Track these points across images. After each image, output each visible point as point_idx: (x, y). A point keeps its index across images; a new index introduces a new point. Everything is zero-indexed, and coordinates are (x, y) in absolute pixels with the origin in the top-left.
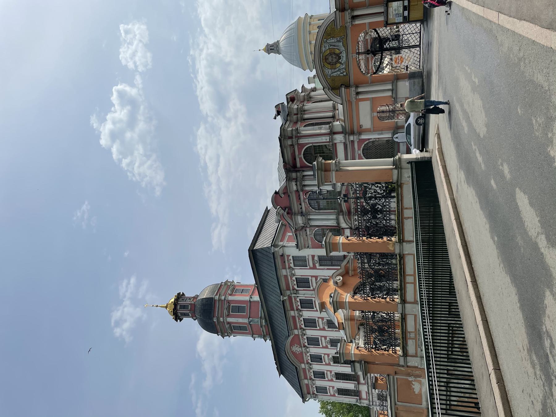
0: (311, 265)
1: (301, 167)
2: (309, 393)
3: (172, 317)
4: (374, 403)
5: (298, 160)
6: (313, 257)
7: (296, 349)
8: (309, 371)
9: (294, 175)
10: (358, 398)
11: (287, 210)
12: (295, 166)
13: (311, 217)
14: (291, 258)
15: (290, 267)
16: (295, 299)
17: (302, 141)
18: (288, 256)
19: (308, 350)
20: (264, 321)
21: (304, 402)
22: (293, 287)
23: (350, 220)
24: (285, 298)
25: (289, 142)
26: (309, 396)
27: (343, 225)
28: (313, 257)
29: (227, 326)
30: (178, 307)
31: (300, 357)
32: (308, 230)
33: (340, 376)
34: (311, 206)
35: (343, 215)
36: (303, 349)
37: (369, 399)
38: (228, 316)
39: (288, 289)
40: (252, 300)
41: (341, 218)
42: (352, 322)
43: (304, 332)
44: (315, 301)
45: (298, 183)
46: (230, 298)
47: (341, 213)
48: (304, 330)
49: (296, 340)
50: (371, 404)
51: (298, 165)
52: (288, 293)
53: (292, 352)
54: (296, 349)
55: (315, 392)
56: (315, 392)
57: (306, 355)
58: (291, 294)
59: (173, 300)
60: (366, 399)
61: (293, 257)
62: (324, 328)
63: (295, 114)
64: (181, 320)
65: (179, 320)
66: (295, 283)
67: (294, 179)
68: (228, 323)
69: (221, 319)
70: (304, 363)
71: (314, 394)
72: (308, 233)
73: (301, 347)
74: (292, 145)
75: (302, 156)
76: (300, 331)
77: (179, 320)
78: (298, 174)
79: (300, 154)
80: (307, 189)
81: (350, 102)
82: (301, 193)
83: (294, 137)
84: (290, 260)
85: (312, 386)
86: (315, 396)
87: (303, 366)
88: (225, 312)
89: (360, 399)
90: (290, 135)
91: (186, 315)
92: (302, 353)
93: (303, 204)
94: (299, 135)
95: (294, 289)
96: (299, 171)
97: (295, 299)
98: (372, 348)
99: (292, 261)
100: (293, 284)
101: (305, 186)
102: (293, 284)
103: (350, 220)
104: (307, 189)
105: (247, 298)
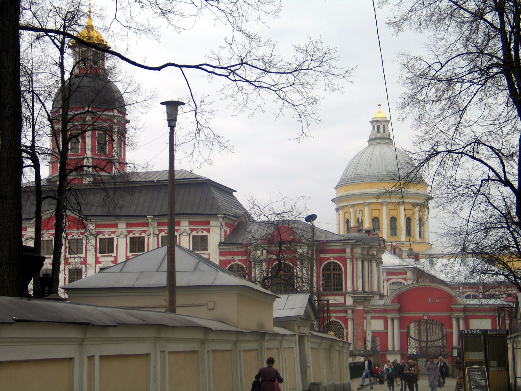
1: (320, 258)
5: (328, 255)
14: (205, 233)
16: (145, 232)
17: (349, 263)
18: (208, 231)
51: (322, 256)
52: (155, 224)
61: (206, 236)
62: (100, 262)
75: (332, 260)
79: (335, 258)
81: (385, 311)
83: (353, 254)
84: (202, 232)
94: (354, 259)
99: (200, 234)
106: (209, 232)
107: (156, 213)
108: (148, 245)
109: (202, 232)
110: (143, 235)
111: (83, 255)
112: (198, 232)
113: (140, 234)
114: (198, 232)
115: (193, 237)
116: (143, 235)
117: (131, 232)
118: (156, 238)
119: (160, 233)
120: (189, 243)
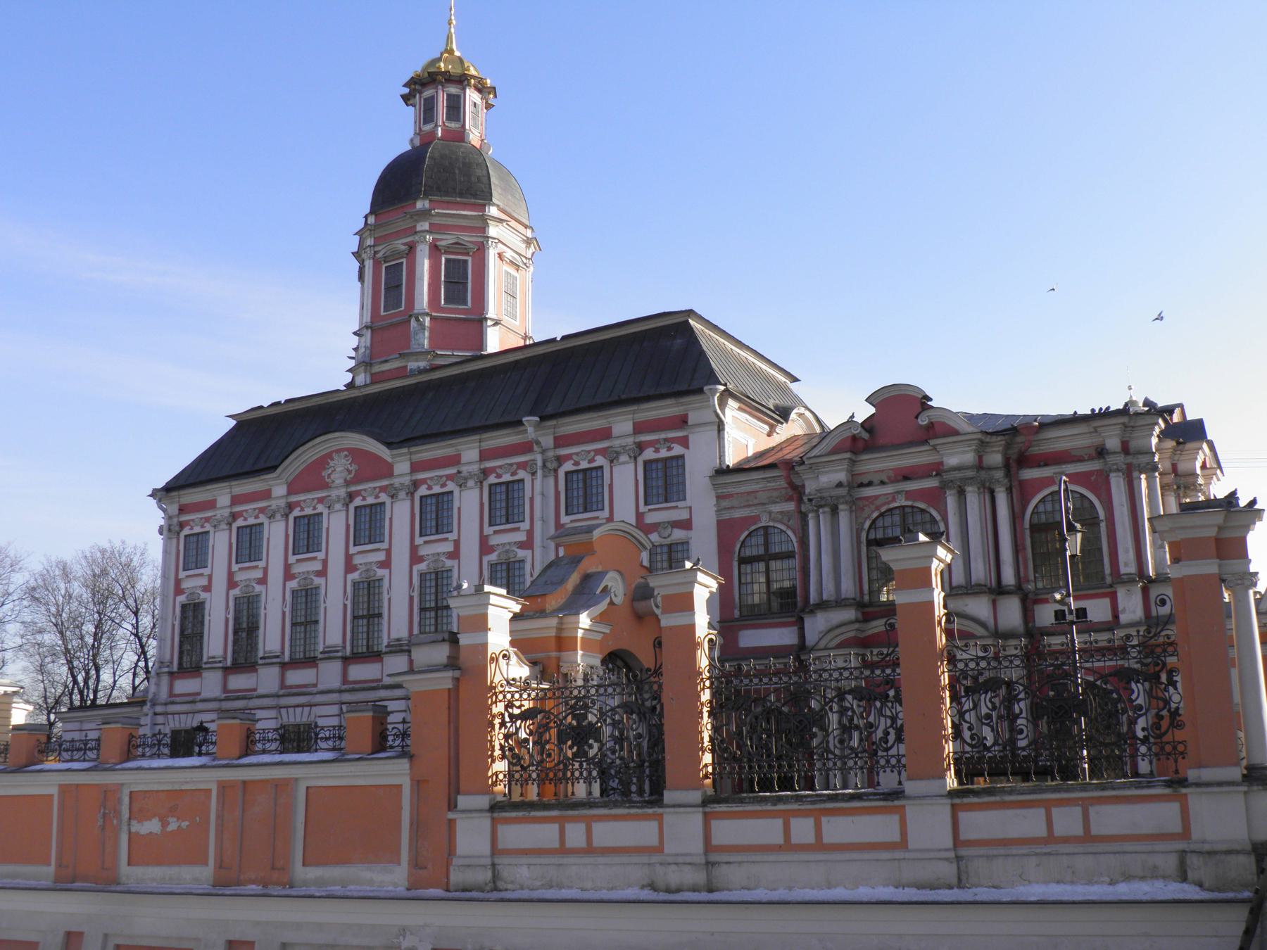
0: (651, 518)
1: (1022, 484)
2: (182, 510)
3: (415, 67)
4: (160, 719)
6: (686, 525)
7: (339, 470)
8: (262, 510)
9: (995, 458)
10: (175, 669)
11: (866, 435)
12: (1025, 460)
13: (844, 518)
14: (677, 450)
15: (641, 447)
16: (522, 466)
18: (684, 442)
19: (338, 506)
20: (422, 364)
21: (154, 494)
22: (569, 457)
23: (839, 646)
24: (530, 430)
25: (1113, 443)
26: (174, 509)
27: (816, 625)
28: (686, 525)
29: (400, 244)
30: (453, 90)
31: (313, 479)
32: (791, 506)
33: (305, 605)
34: (882, 515)
35: (857, 621)
36: (342, 492)
37: (173, 703)
38: (435, 249)
39: (560, 442)
40: (489, 323)
41: (850, 614)
42: (553, 643)
43: (402, 495)
44: (518, 529)
45: (970, 474)
46: (492, 254)
47: (860, 616)
48: (411, 494)
49: (370, 469)
50: (159, 709)
51: (1029, 474)
52: (547, 441)
53: (329, 456)
54: (339, 470)
55: (186, 531)
56: (186, 531)
57: (321, 500)
58: (543, 452)
59: (473, 72)
60: (171, 694)
61: (682, 457)
63: (1174, 467)
64: (406, 99)
65: (406, 90)
66: (584, 465)
67: (980, 458)
68: (411, 248)
69: (425, 226)
70: (290, 493)
71: (182, 525)
72: (776, 508)
73: (347, 483)
74: (1101, 452)
76: (407, 480)
77: (406, 90)
78: (999, 474)
80: (951, 501)
82: (931, 483)
83: (1129, 459)
84: (670, 449)
85: (207, 520)
86: (170, 530)
87: (280, 490)
88: (447, 240)
89: (171, 674)
90: (1133, 445)
91: (428, 113)
92: (325, 486)
93: (889, 489)
95: (560, 460)
96: (1008, 474)
97: (522, 466)
98: (509, 705)
99: (664, 453)
100: (581, 457)
101: (961, 493)
102: (581, 457)
103: (839, 646)
104: (951, 501)
105: (492, 312)
106: (687, 447)
107: (550, 410)
108: (532, 499)
109: (670, 449)
110: (521, 474)
111: (385, 545)
112: (657, 451)
113: (512, 475)
114: (657, 451)
115: (647, 464)
116: (521, 474)
117: (493, 470)
118: (551, 481)
119: (560, 465)
120: (637, 481)
